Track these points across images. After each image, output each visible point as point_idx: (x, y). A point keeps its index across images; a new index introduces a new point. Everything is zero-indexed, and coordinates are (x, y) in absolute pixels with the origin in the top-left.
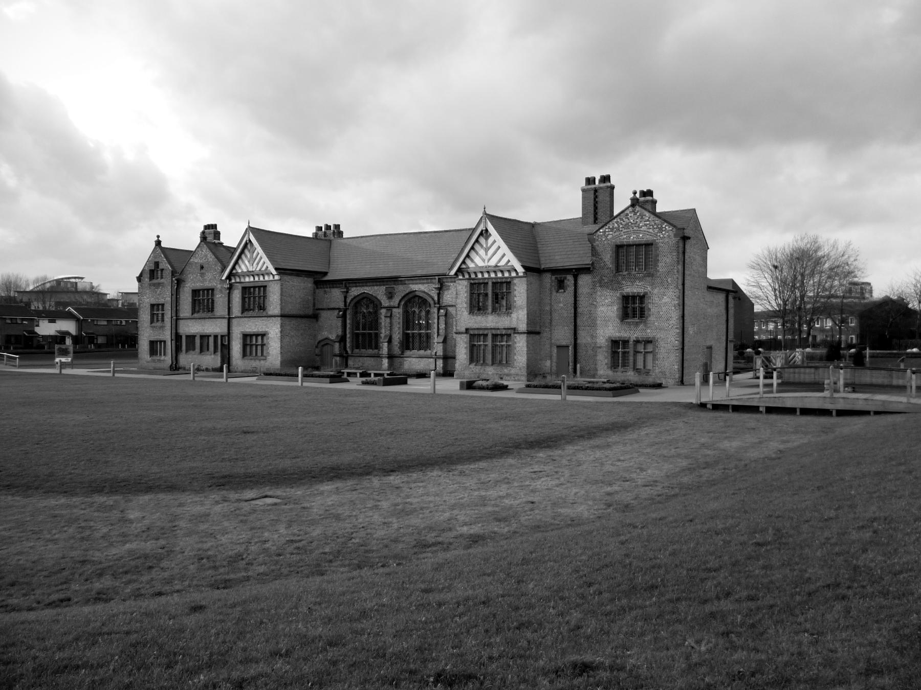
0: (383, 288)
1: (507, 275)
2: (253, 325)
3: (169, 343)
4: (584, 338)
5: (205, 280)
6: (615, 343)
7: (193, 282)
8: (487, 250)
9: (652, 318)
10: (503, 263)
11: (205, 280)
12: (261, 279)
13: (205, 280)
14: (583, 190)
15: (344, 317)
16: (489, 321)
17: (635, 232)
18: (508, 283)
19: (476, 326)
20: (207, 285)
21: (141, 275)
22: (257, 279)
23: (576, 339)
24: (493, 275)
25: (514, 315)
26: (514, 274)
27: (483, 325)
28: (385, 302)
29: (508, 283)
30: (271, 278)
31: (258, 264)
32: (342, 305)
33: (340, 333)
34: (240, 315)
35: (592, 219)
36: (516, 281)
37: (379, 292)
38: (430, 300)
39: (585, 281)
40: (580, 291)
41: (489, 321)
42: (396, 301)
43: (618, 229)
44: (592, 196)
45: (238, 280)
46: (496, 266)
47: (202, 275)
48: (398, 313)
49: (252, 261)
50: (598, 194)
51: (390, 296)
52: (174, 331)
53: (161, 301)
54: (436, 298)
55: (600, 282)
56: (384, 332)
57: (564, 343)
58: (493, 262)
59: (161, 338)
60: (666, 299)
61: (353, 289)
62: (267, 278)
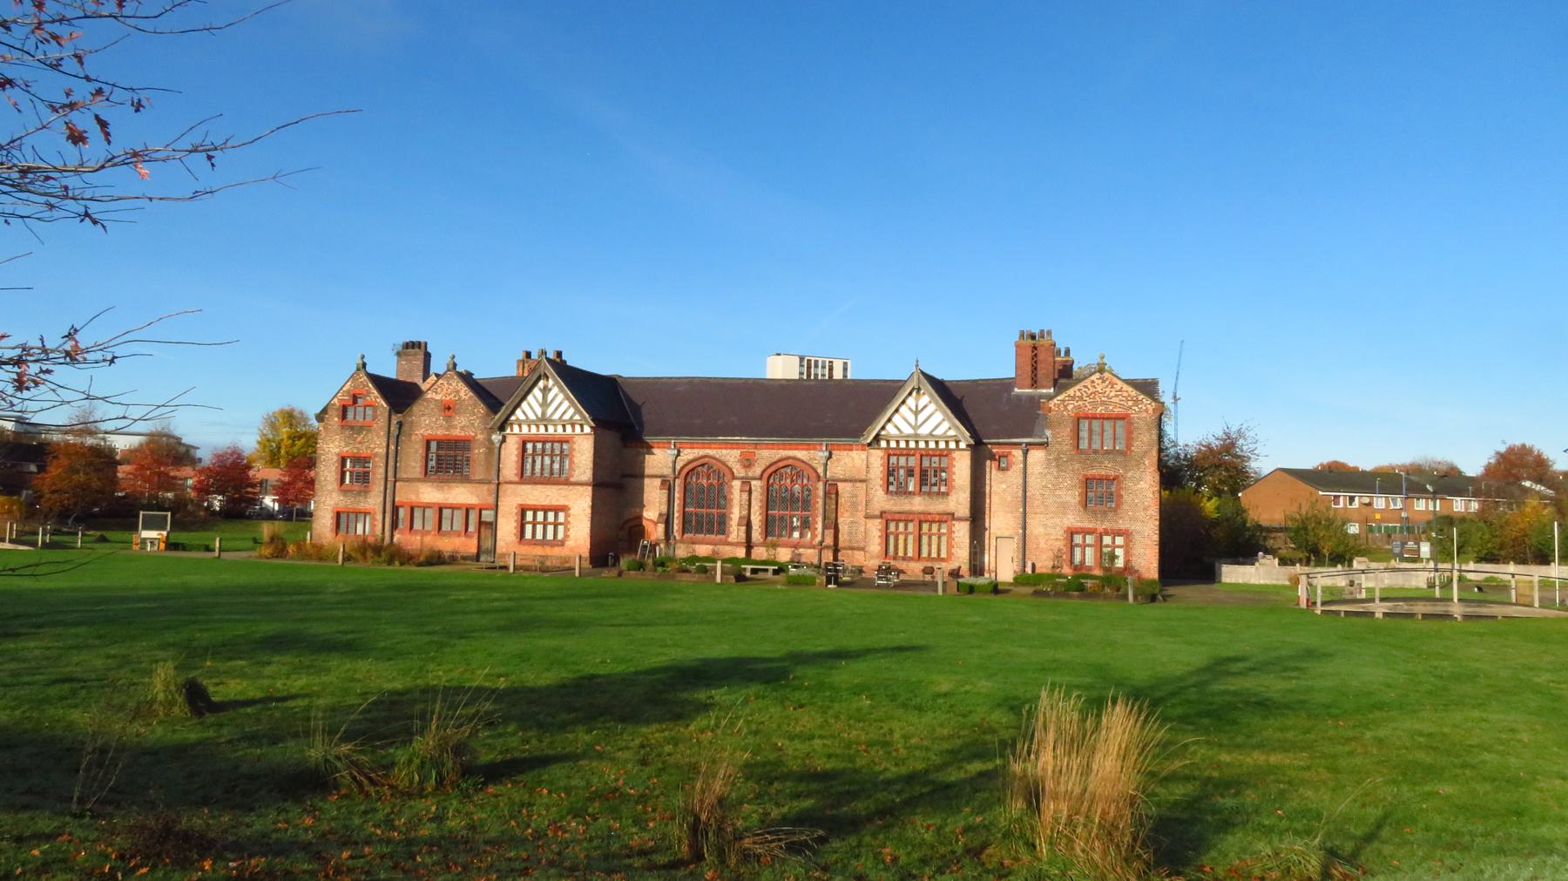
0: (736, 453)
1: (942, 445)
3: (379, 517)
4: (1036, 527)
5: (455, 427)
7: (426, 423)
8: (916, 413)
9: (1125, 507)
10: (938, 432)
11: (455, 427)
12: (560, 429)
13: (450, 427)
14: (1017, 346)
15: (670, 490)
16: (918, 504)
17: (1103, 403)
18: (945, 454)
19: (895, 509)
20: (457, 432)
21: (324, 411)
22: (551, 429)
23: (1024, 528)
24: (922, 445)
25: (953, 498)
26: (952, 445)
27: (907, 508)
28: (738, 470)
29: (945, 454)
32: (668, 471)
33: (664, 509)
34: (516, 479)
35: (1029, 381)
36: (956, 455)
38: (808, 471)
39: (1036, 456)
40: (1029, 471)
41: (918, 504)
42: (757, 470)
43: (1081, 398)
44: (1029, 353)
46: (931, 434)
47: (448, 418)
48: (757, 485)
51: (748, 463)
52: (389, 499)
53: (364, 452)
55: (1057, 459)
56: (736, 514)
57: (1006, 534)
58: (924, 431)
59: (362, 506)
60: (1142, 485)
61: (687, 451)
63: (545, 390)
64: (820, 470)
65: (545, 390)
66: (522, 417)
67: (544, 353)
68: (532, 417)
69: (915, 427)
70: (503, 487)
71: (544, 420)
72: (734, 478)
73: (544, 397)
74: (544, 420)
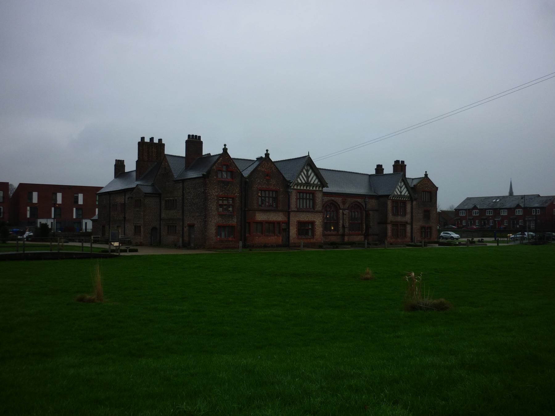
0: (340, 199)
2: (305, 217)
6: (422, 227)
8: (401, 188)
12: (311, 189)
16: (399, 219)
18: (404, 203)
22: (308, 188)
28: (342, 206)
29: (404, 203)
30: (317, 189)
31: (312, 179)
37: (339, 200)
42: (347, 206)
45: (295, 187)
49: (308, 177)
50: (399, 166)
51: (344, 203)
54: (364, 206)
58: (403, 194)
62: (314, 189)
63: (307, 171)
64: (364, 206)
65: (307, 171)
66: (300, 182)
67: (152, 139)
68: (304, 182)
69: (401, 192)
70: (292, 214)
71: (308, 184)
72: (340, 209)
73: (307, 173)
74: (308, 184)
